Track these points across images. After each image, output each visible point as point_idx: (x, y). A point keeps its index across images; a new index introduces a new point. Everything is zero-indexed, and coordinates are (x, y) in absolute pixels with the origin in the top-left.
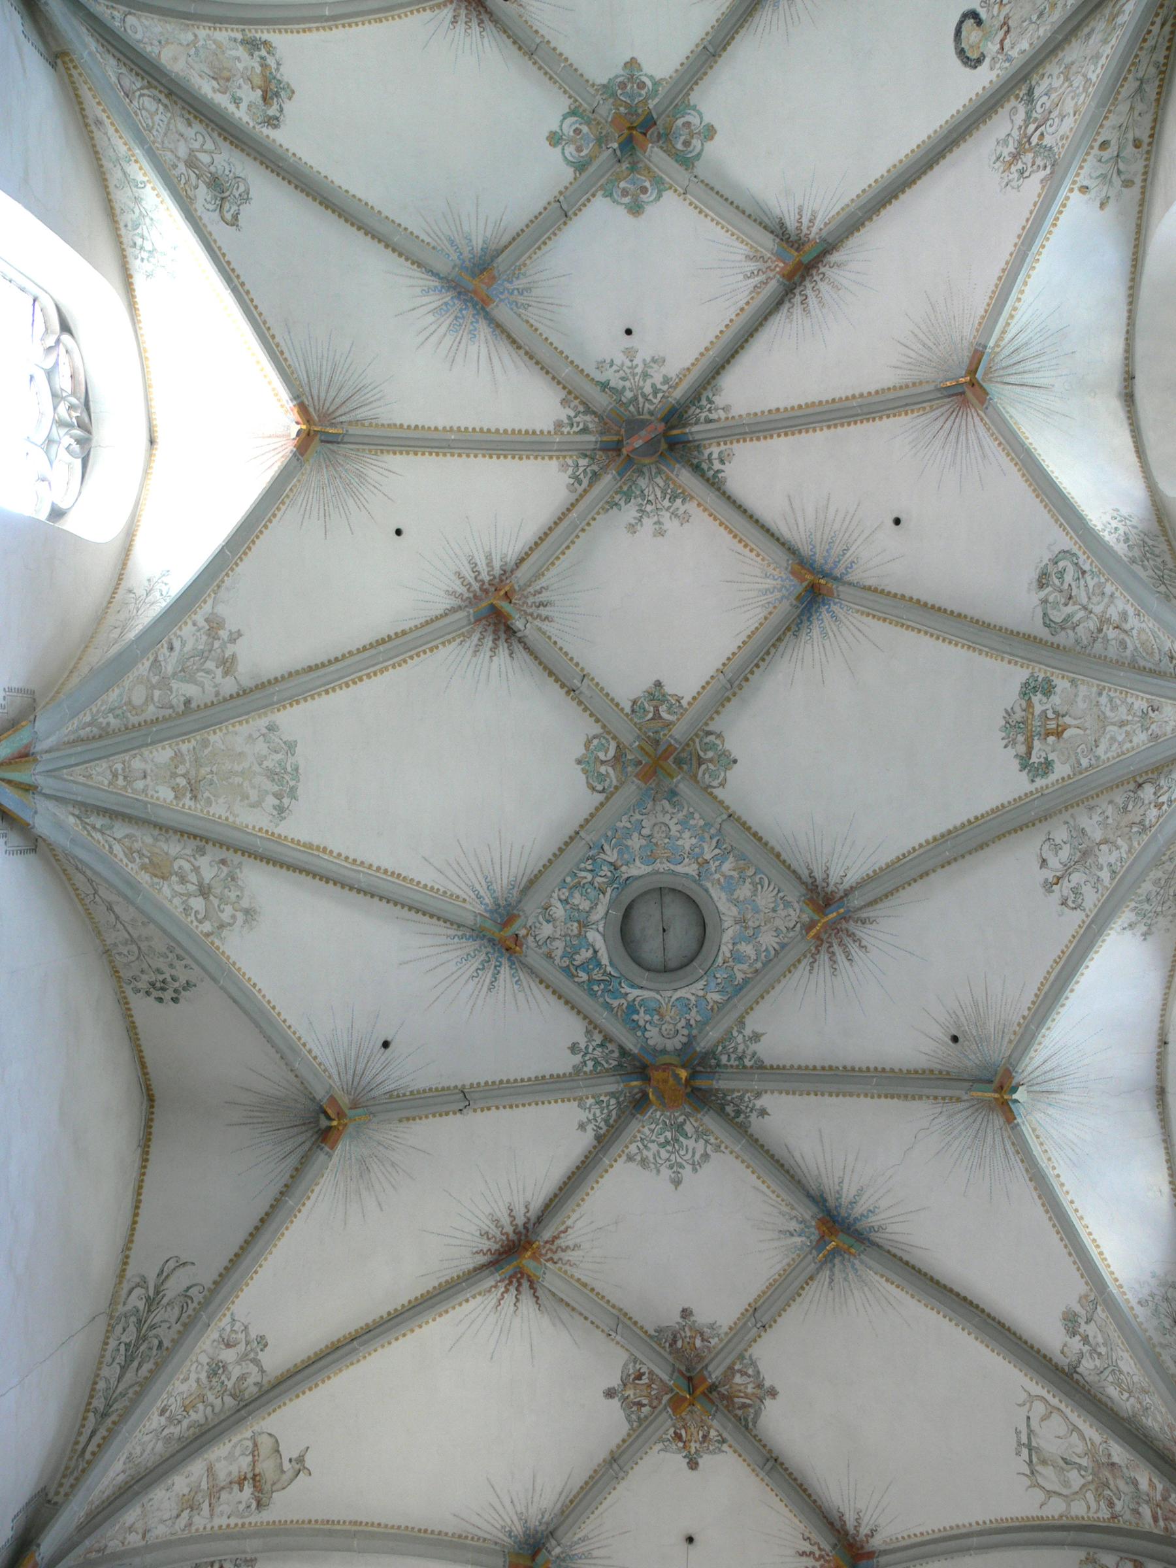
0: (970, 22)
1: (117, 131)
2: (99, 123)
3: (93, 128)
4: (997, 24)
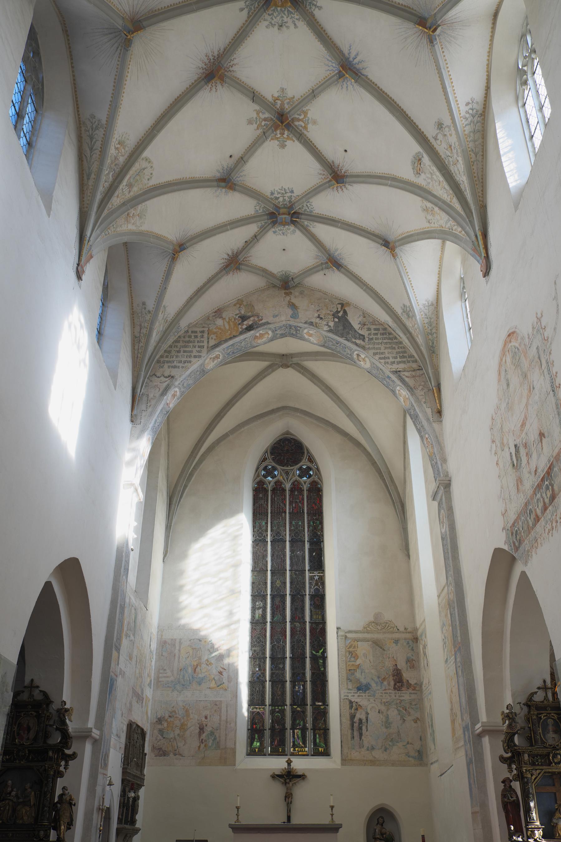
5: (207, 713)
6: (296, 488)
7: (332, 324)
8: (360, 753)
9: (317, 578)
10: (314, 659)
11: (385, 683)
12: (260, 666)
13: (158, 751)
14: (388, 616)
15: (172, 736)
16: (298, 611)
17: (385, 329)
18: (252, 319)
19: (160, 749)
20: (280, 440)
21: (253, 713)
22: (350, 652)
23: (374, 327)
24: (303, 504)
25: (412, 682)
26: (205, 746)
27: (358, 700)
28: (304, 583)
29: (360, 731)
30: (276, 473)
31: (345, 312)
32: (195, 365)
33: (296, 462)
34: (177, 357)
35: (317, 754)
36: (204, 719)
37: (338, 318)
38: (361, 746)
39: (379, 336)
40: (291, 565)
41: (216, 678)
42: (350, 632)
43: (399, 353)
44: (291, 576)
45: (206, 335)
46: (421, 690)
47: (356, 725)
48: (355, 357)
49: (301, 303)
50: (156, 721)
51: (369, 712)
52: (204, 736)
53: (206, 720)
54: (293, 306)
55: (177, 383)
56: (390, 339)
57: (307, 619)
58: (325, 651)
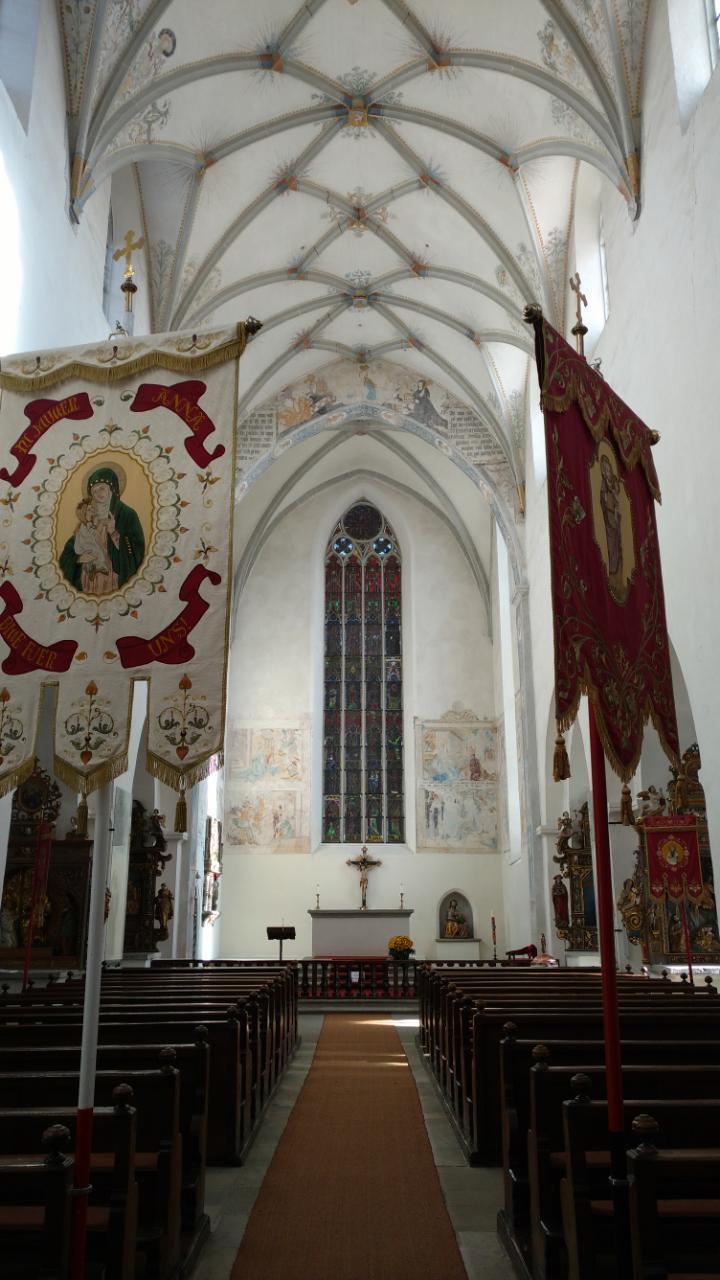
0: (169, 51)
1: (626, 63)
2: (634, 69)
3: (638, 66)
4: (155, 55)
5: (282, 803)
6: (373, 563)
7: (412, 406)
9: (393, 664)
10: (390, 747)
11: (463, 773)
12: (334, 755)
14: (467, 705)
16: (374, 697)
17: (470, 413)
18: (324, 399)
19: (235, 838)
20: (356, 507)
21: (327, 802)
22: (427, 742)
23: (459, 410)
24: (380, 583)
25: (490, 772)
27: (434, 790)
28: (380, 669)
30: (350, 546)
31: (427, 392)
32: (264, 455)
33: (372, 533)
34: (244, 445)
35: (391, 840)
37: (419, 399)
38: (437, 834)
39: (463, 422)
40: (367, 650)
41: (290, 768)
42: (427, 721)
43: (484, 442)
44: (366, 661)
45: (274, 420)
46: (497, 780)
47: (432, 814)
48: (437, 443)
49: (379, 380)
51: (445, 801)
52: (278, 825)
54: (369, 384)
55: (245, 477)
56: (475, 425)
57: (383, 707)
58: (401, 740)
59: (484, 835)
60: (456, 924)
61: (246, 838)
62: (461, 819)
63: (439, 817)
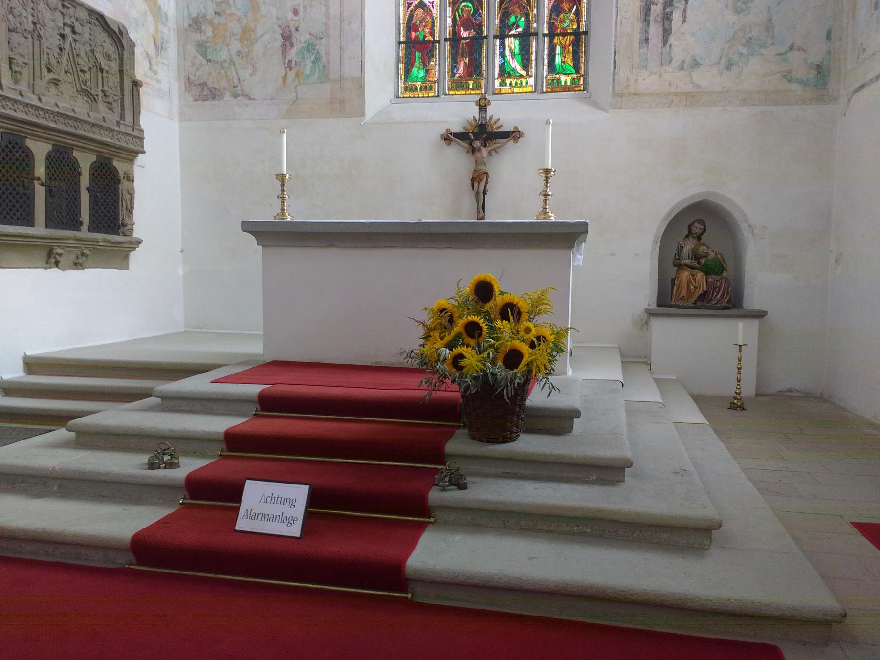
8: (660, 76)
13: (200, 89)
15: (224, 55)
19: (203, 85)
26: (297, 75)
29: (667, 23)
36: (290, 15)
38: (665, 60)
50: (190, 25)
52: (292, 54)
53: (296, 18)
59: (794, 56)
60: (700, 275)
61: (224, 83)
62: (731, 18)
63: (676, 16)
